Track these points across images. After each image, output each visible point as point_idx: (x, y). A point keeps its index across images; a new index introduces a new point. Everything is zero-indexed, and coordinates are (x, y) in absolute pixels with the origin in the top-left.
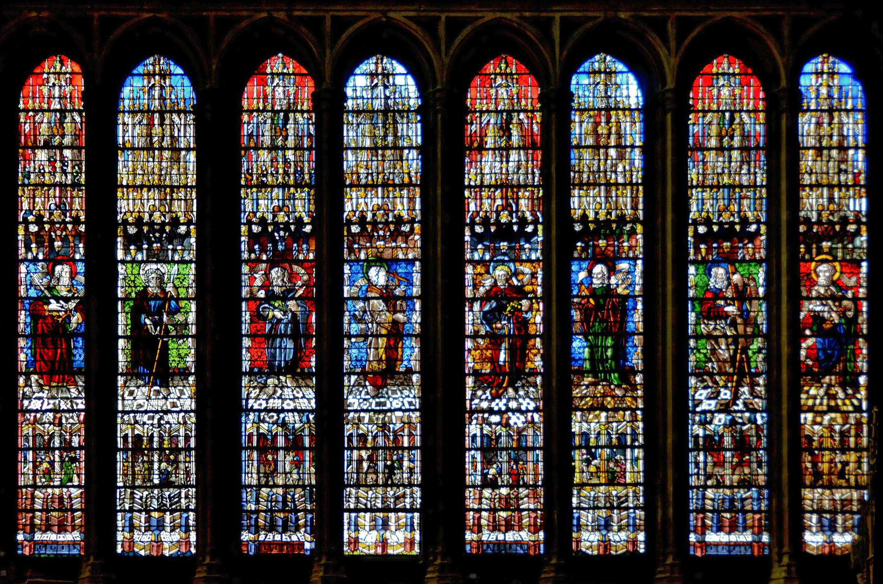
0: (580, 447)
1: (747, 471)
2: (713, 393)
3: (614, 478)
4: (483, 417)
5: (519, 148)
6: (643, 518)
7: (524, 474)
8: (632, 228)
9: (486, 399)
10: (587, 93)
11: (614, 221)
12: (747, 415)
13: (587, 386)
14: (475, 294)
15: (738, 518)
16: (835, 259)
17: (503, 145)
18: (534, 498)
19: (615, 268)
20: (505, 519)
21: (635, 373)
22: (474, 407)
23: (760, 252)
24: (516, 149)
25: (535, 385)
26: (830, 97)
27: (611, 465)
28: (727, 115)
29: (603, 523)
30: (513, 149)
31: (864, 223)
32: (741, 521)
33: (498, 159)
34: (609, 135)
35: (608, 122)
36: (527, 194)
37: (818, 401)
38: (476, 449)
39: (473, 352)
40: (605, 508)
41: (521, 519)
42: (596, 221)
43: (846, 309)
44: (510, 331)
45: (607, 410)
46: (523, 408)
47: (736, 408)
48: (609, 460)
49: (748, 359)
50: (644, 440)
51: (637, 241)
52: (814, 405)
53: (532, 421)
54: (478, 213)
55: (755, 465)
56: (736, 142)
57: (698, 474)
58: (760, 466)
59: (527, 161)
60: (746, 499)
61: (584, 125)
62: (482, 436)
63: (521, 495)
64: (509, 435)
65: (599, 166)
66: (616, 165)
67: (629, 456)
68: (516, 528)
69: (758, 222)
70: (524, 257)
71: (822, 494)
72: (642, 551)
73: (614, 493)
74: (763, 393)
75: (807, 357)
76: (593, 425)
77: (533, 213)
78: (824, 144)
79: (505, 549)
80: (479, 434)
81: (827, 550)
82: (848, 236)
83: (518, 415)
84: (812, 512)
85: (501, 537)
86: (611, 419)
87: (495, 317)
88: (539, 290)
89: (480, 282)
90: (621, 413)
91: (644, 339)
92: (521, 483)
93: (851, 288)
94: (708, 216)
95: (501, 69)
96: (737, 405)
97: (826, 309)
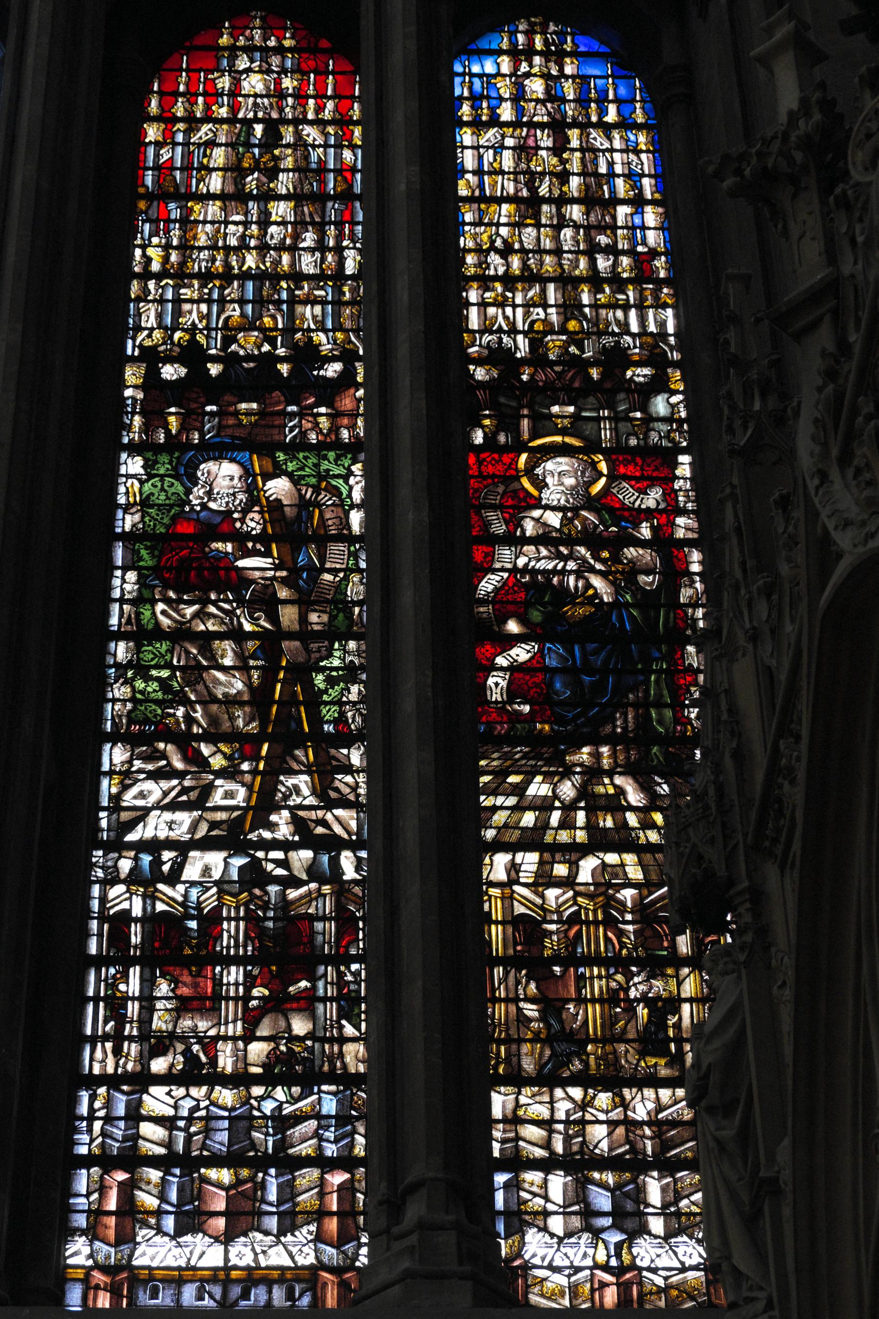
1: (300, 1026)
2: (185, 791)
12: (307, 854)
15: (263, 1186)
16: (592, 446)
23: (352, 427)
26: (553, 96)
28: (259, 129)
31: (675, 365)
32: (272, 1195)
37: (555, 817)
43: (634, 570)
47: (267, 835)
49: (314, 700)
52: (542, 826)
55: (332, 1009)
56: (284, 183)
57: (118, 1038)
58: (348, 1013)
60: (298, 1119)
69: (347, 356)
71: (583, 1106)
74: (362, 791)
75: (513, 693)
78: (543, 191)
81: (610, 1297)
82: (629, 391)
84: (547, 1166)
93: (648, 514)
94: (193, 341)
96: (272, 827)
97: (571, 565)
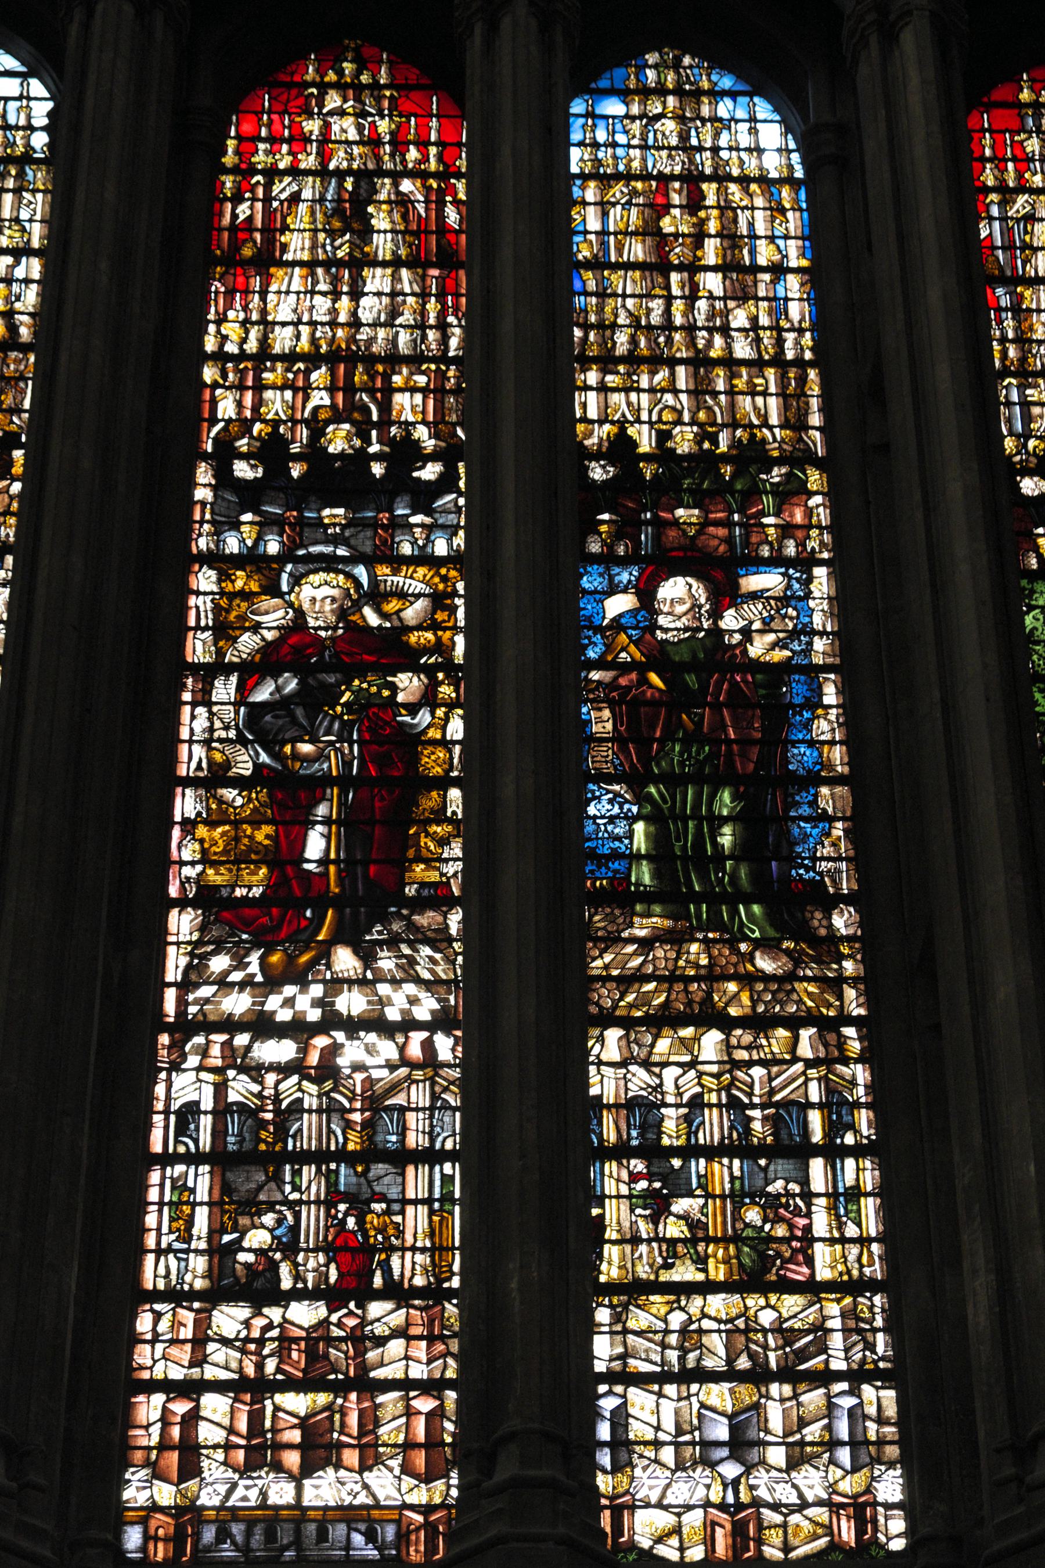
0: (621, 1152)
3: (764, 1263)
4: (227, 1045)
5: (396, 263)
6: (891, 1411)
7: (392, 1249)
8: (789, 476)
9: (246, 983)
10: (621, 139)
11: (725, 458)
13: (646, 945)
14: (220, 653)
17: (340, 254)
18: (431, 1339)
19: (737, 586)
20: (304, 1423)
21: (830, 903)
22: (193, 1009)
24: (384, 264)
25: (439, 939)
27: (753, 1215)
29: (721, 1431)
30: (375, 263)
33: (323, 287)
34: (699, 237)
35: (694, 204)
36: (421, 380)
38: (194, 1159)
39: (202, 831)
40: (731, 1375)
41: (370, 1421)
42: (663, 453)
44: (347, 765)
45: (726, 1024)
46: (393, 1014)
48: (739, 1197)
50: (880, 1123)
51: (809, 512)
53: (430, 1059)
54: (245, 426)
59: (423, 296)
61: (616, 212)
62: (222, 1110)
63: (379, 1329)
64: (330, 1109)
65: (667, 312)
66: (726, 313)
67: (818, 1180)
68: (351, 1457)
70: (406, 549)
72: (897, 1545)
73: (767, 1318)
76: (670, 1074)
77: (437, 428)
79: (297, 1542)
80: (207, 1104)
83: (372, 1037)
85: (282, 1493)
86: (742, 1055)
87: (294, 721)
88: (460, 640)
89: (242, 618)
90: (782, 1033)
91: (853, 793)
92: (378, 1281)
95: (340, 73)
